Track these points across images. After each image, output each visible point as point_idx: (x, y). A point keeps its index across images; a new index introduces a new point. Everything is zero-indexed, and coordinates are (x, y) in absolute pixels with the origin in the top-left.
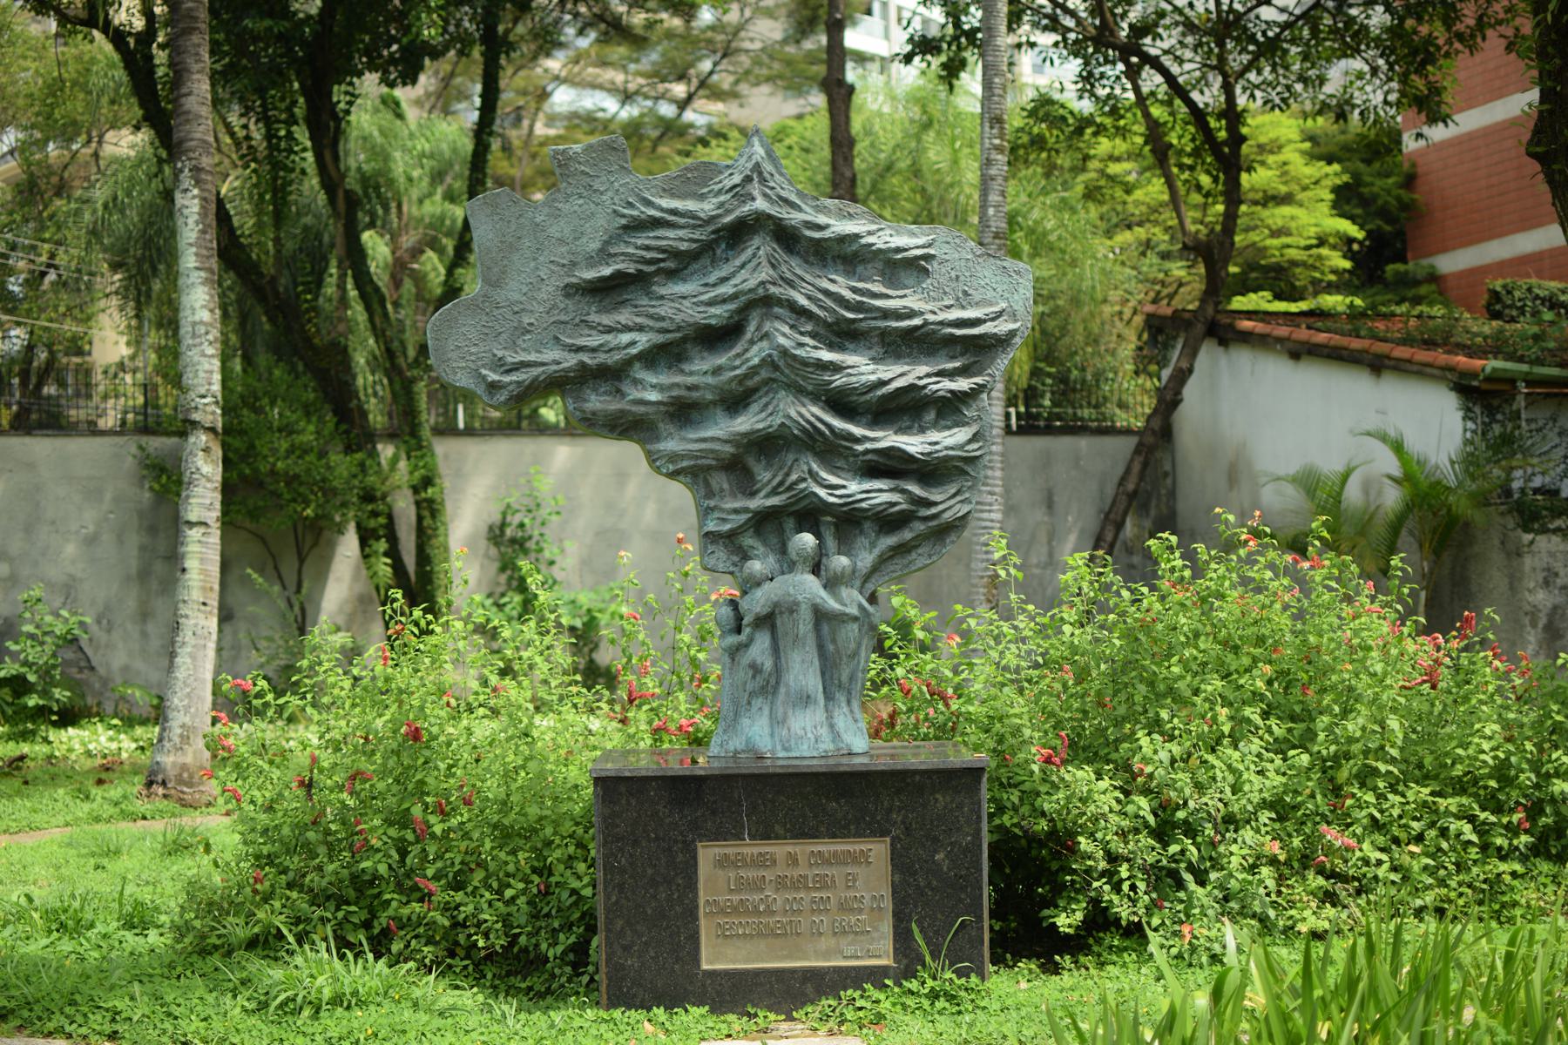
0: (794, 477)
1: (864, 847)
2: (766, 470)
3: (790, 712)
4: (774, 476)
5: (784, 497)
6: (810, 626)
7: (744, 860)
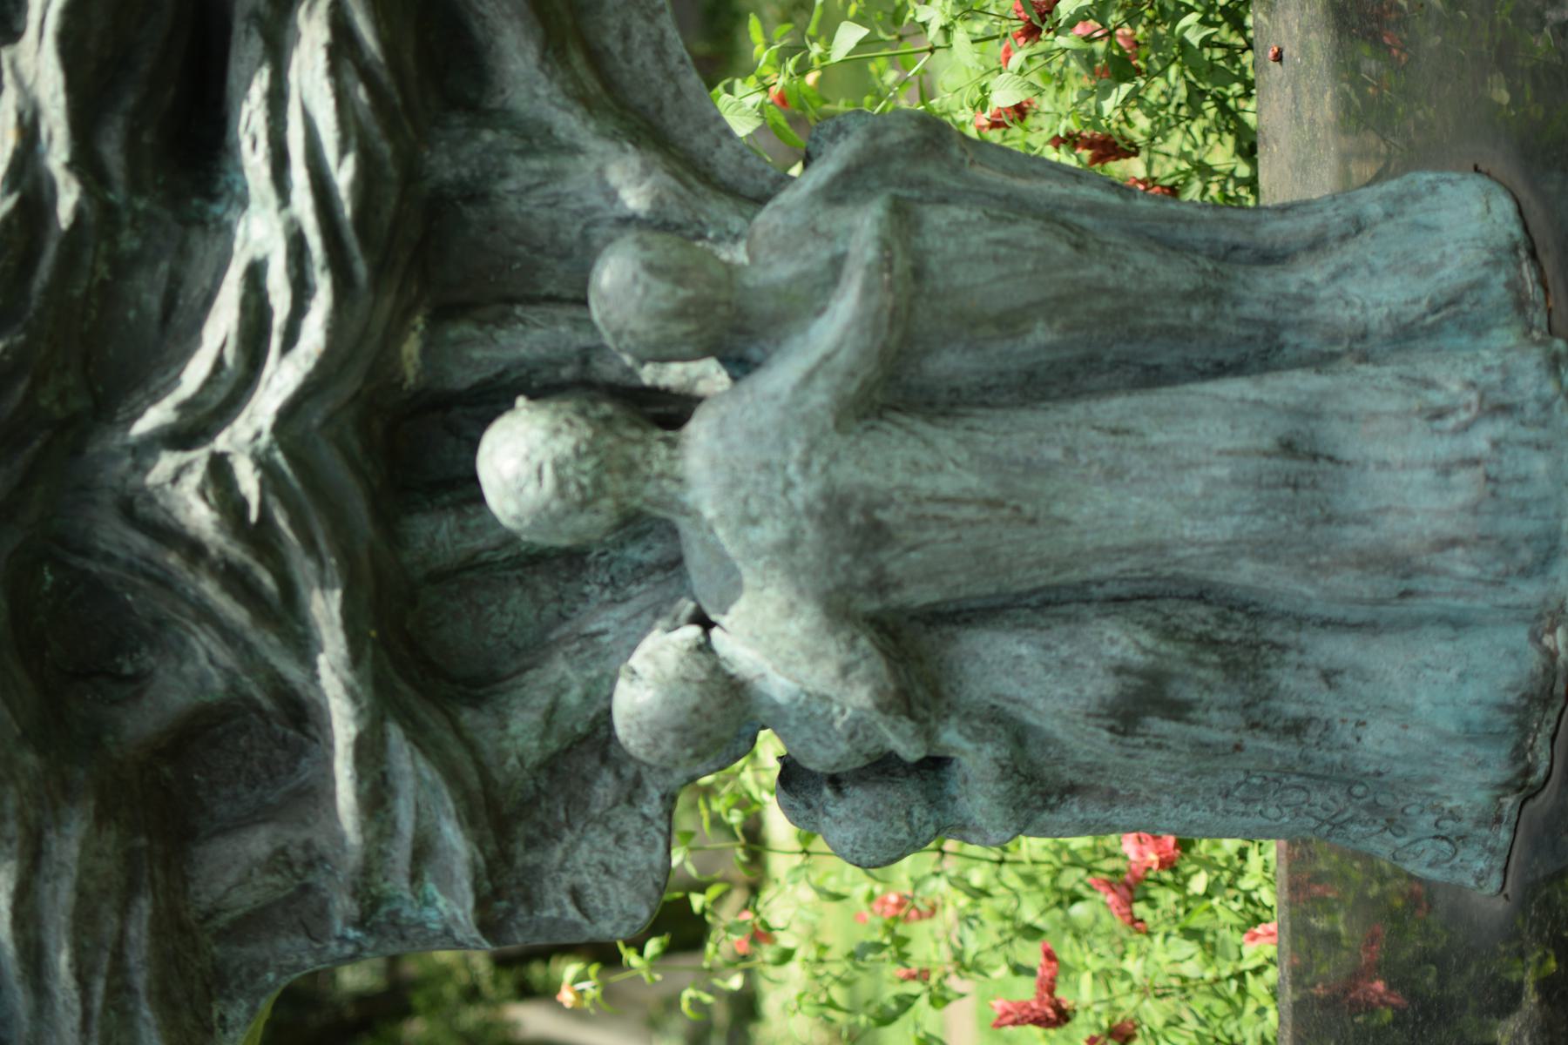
0: (200, 516)
2: (181, 652)
3: (1356, 536)
4: (206, 615)
5: (303, 567)
6: (945, 439)
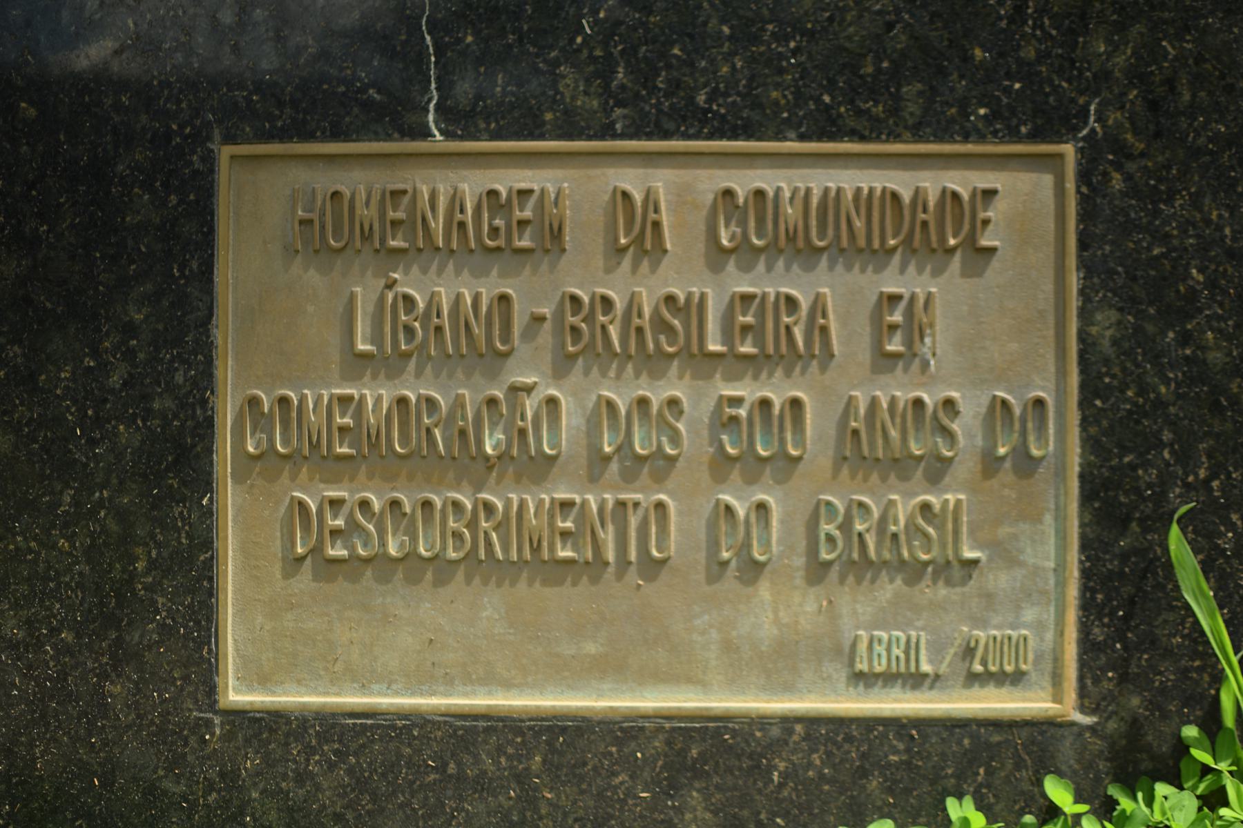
1: (962, 182)
7: (416, 223)
